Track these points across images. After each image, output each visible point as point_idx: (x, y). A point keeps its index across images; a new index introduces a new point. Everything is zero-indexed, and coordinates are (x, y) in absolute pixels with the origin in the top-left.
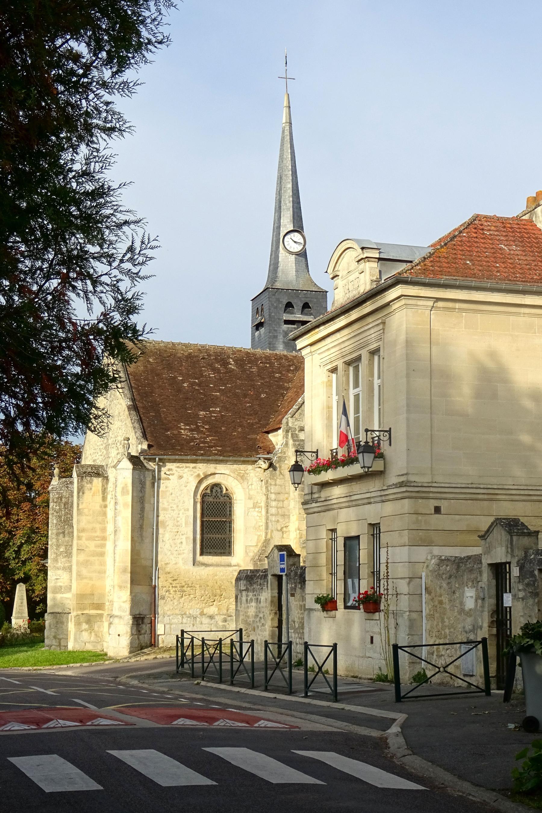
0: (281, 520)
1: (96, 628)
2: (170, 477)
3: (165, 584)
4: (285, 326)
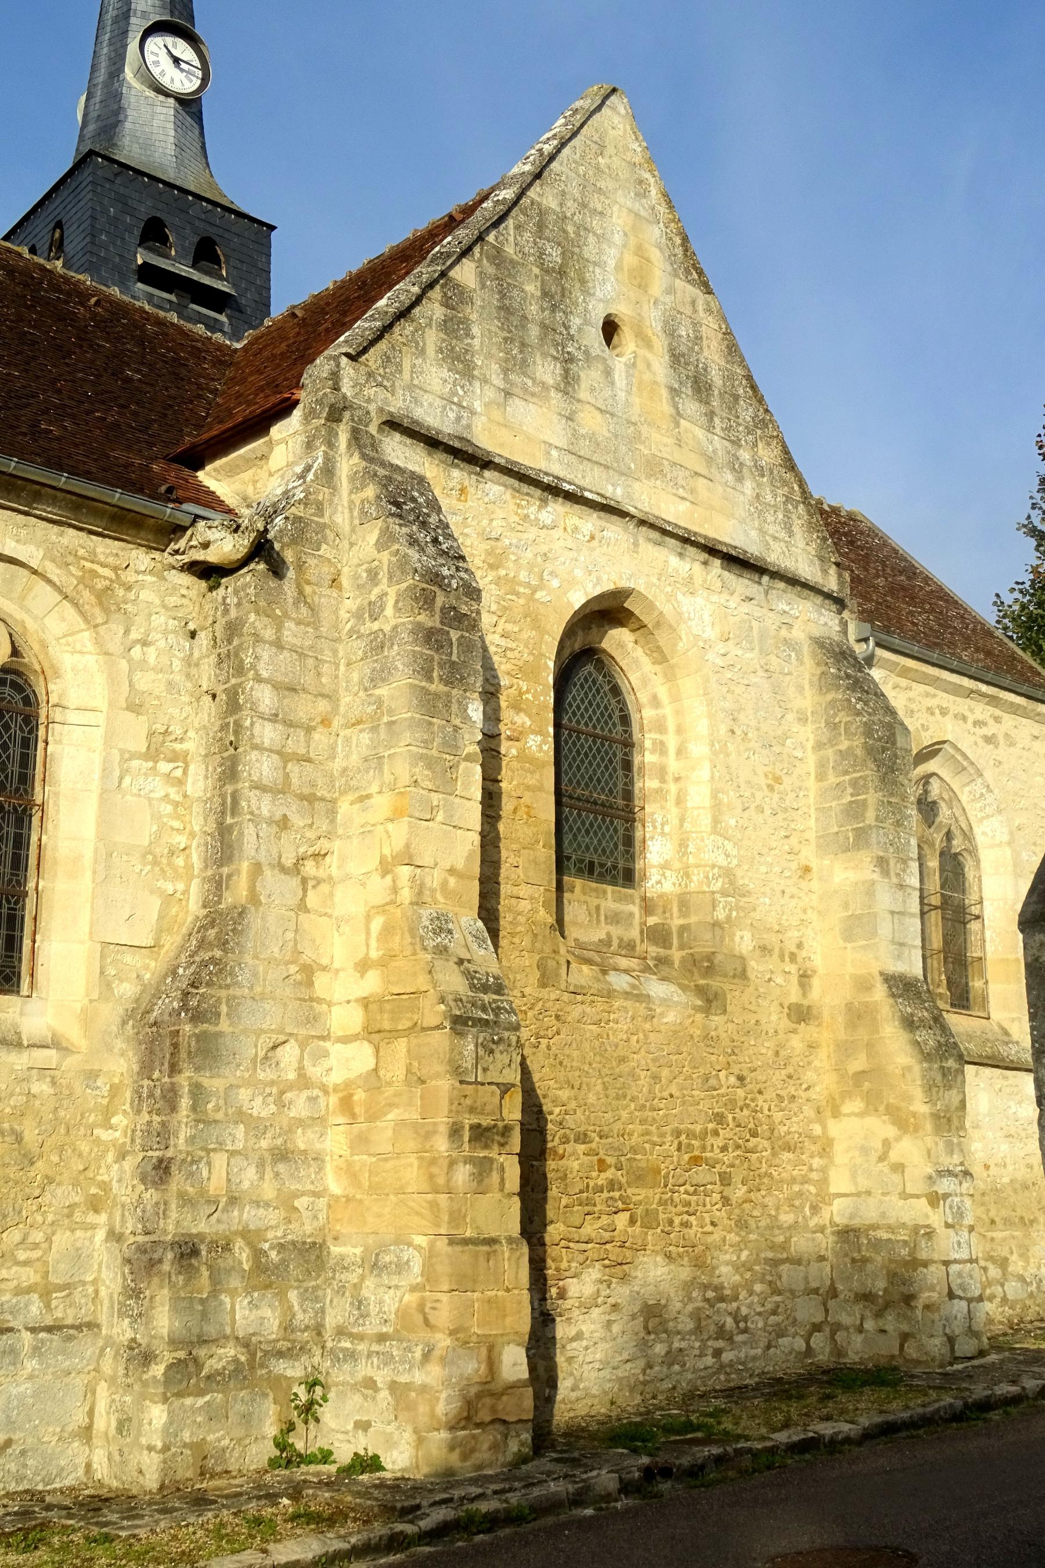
0: (298, 821)
4: (140, 285)
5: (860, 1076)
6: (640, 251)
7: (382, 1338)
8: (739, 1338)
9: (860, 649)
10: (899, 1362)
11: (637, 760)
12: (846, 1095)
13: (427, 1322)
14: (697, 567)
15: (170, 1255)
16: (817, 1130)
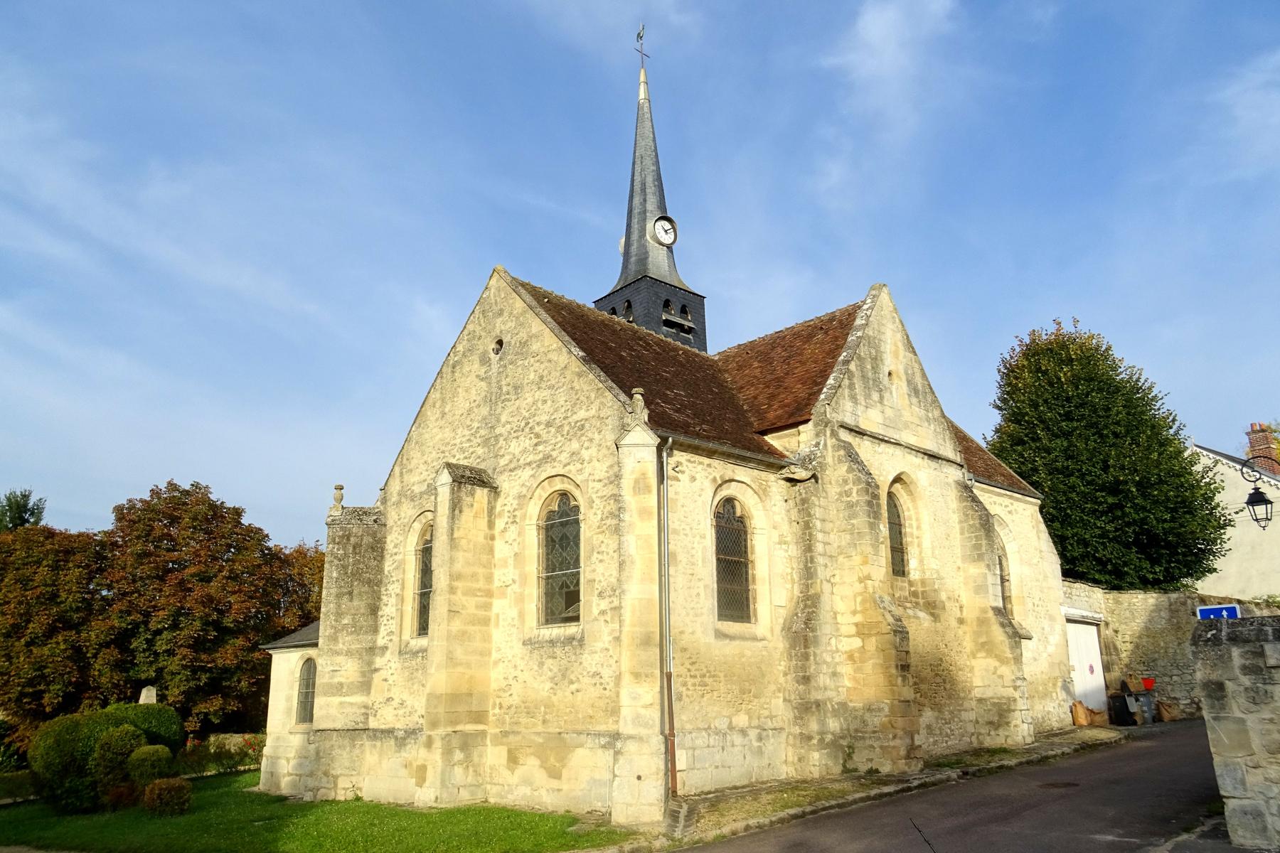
0: (829, 564)
1: (476, 759)
2: (680, 476)
3: (683, 671)
5: (983, 644)
6: (896, 345)
7: (875, 732)
8: (952, 737)
9: (969, 482)
10: (1005, 746)
11: (903, 531)
12: (979, 650)
13: (892, 726)
14: (921, 460)
15: (814, 706)
16: (968, 663)
